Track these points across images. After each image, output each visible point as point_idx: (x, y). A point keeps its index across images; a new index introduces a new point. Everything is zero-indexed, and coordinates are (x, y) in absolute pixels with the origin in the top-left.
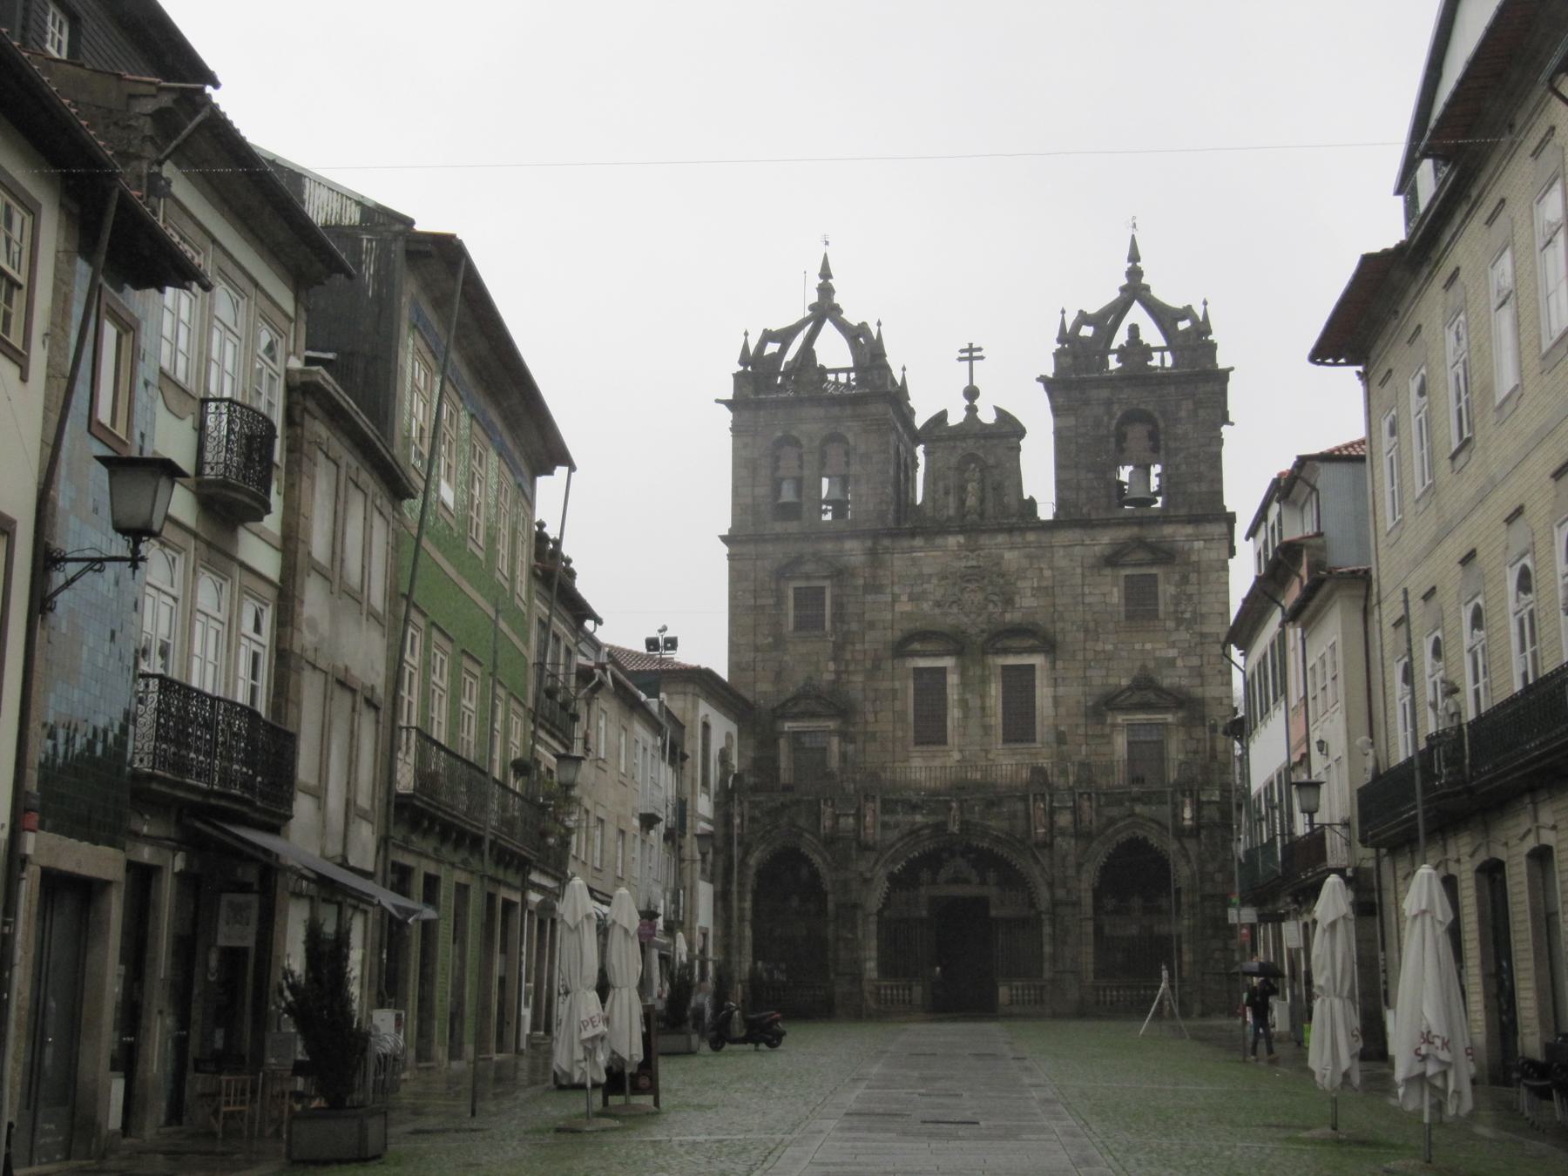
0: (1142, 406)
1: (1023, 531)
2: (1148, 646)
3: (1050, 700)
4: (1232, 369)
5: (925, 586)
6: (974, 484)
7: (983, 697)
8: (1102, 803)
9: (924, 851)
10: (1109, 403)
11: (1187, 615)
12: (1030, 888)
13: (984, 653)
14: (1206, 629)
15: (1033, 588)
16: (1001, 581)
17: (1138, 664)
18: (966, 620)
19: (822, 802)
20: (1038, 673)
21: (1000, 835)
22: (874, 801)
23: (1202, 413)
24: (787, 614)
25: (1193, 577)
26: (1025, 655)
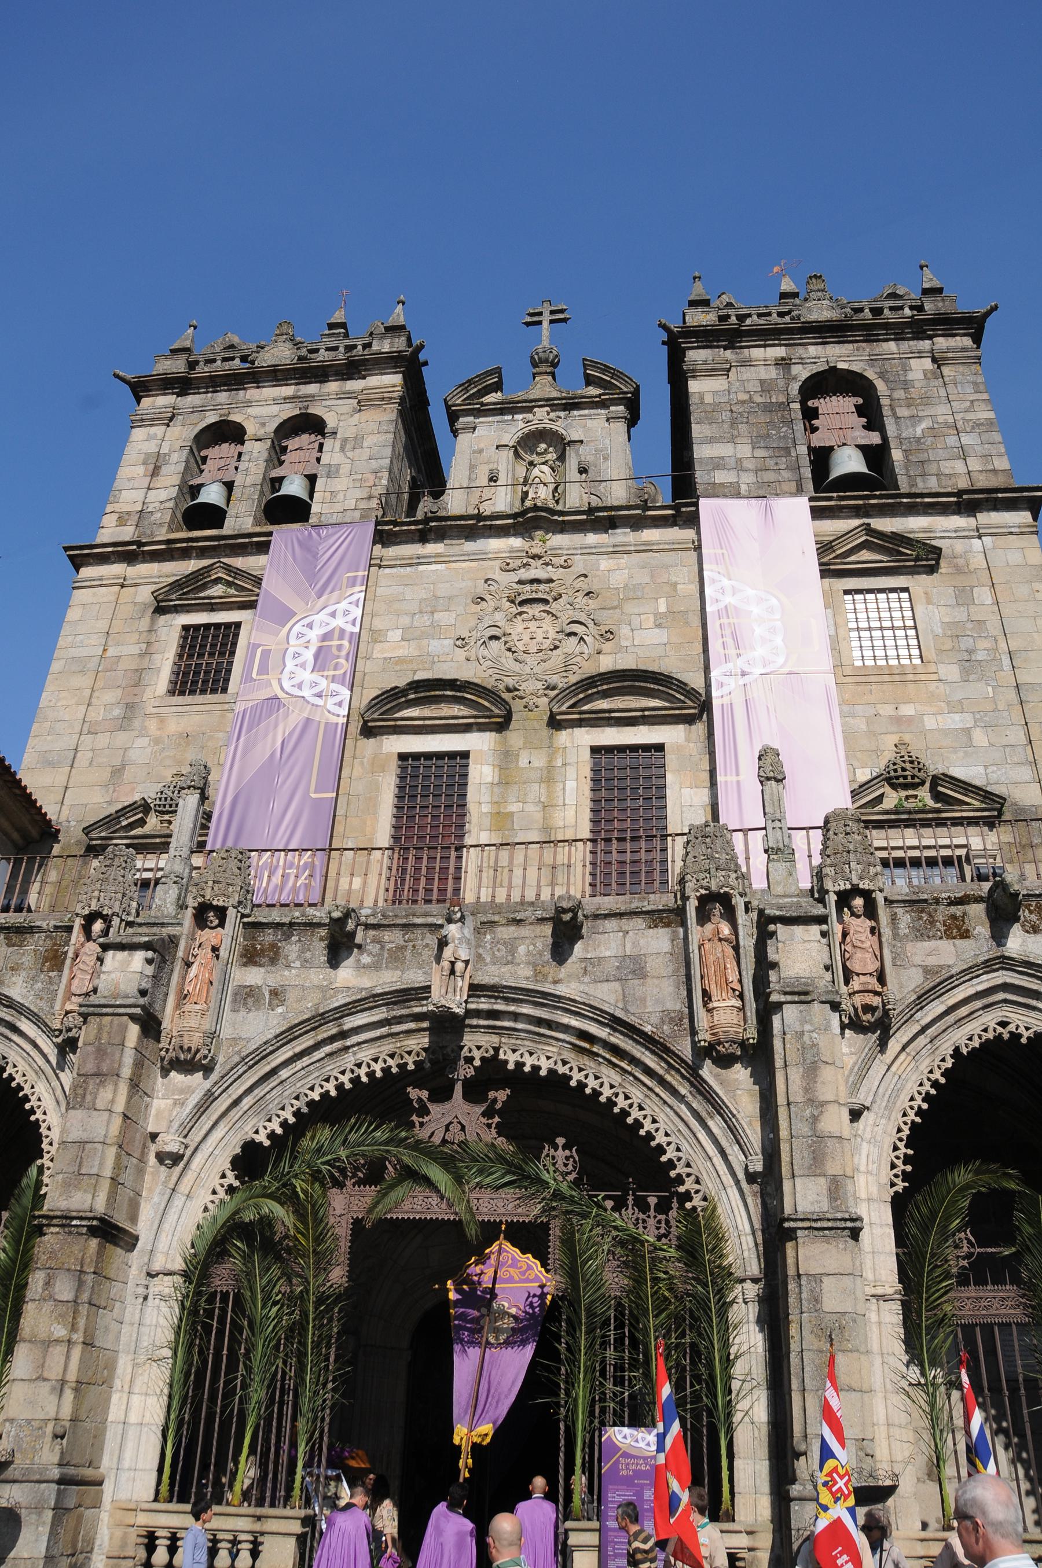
0: (841, 366)
1: (637, 523)
2: (908, 710)
3: (701, 812)
4: (995, 308)
5: (436, 614)
6: (545, 468)
7: (546, 807)
8: (903, 928)
9: (356, 1081)
10: (784, 363)
11: (981, 656)
12: (687, 1196)
13: (555, 723)
14: (1024, 678)
15: (657, 615)
16: (593, 604)
17: (890, 741)
18: (517, 667)
19: (78, 922)
20: (671, 759)
21: (593, 1029)
22: (222, 925)
23: (946, 370)
24: (159, 670)
25: (983, 595)
26: (643, 729)
